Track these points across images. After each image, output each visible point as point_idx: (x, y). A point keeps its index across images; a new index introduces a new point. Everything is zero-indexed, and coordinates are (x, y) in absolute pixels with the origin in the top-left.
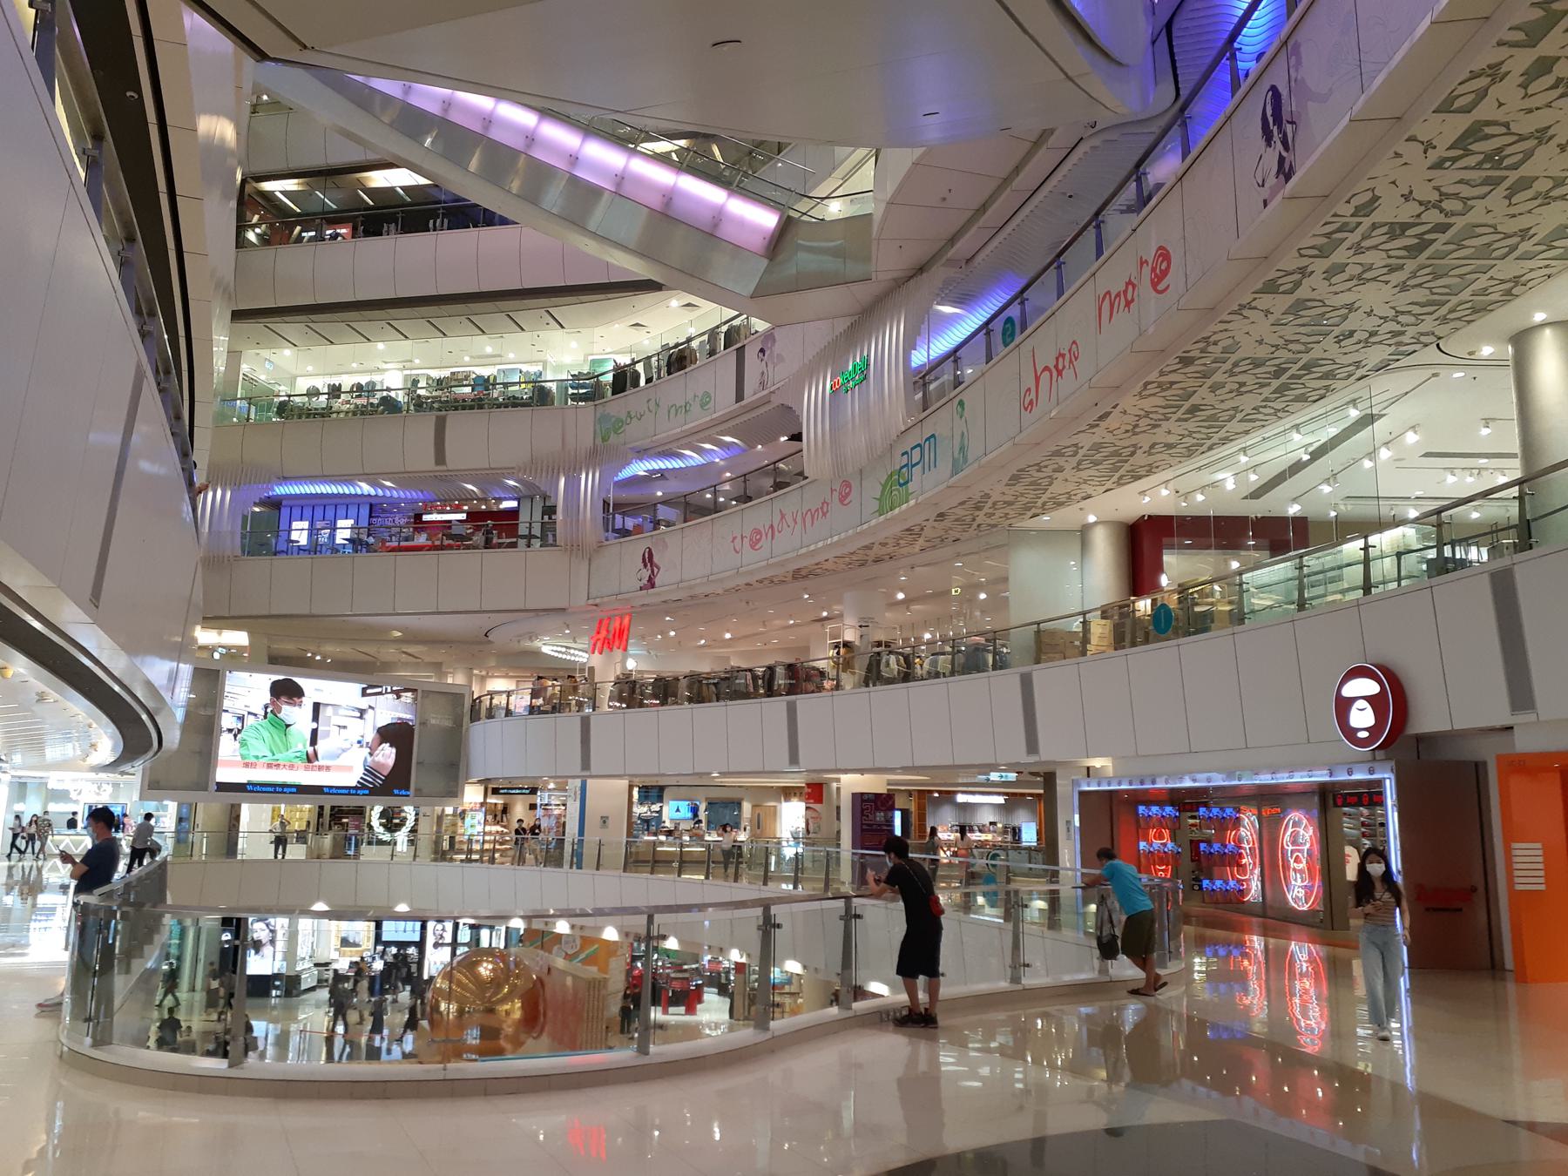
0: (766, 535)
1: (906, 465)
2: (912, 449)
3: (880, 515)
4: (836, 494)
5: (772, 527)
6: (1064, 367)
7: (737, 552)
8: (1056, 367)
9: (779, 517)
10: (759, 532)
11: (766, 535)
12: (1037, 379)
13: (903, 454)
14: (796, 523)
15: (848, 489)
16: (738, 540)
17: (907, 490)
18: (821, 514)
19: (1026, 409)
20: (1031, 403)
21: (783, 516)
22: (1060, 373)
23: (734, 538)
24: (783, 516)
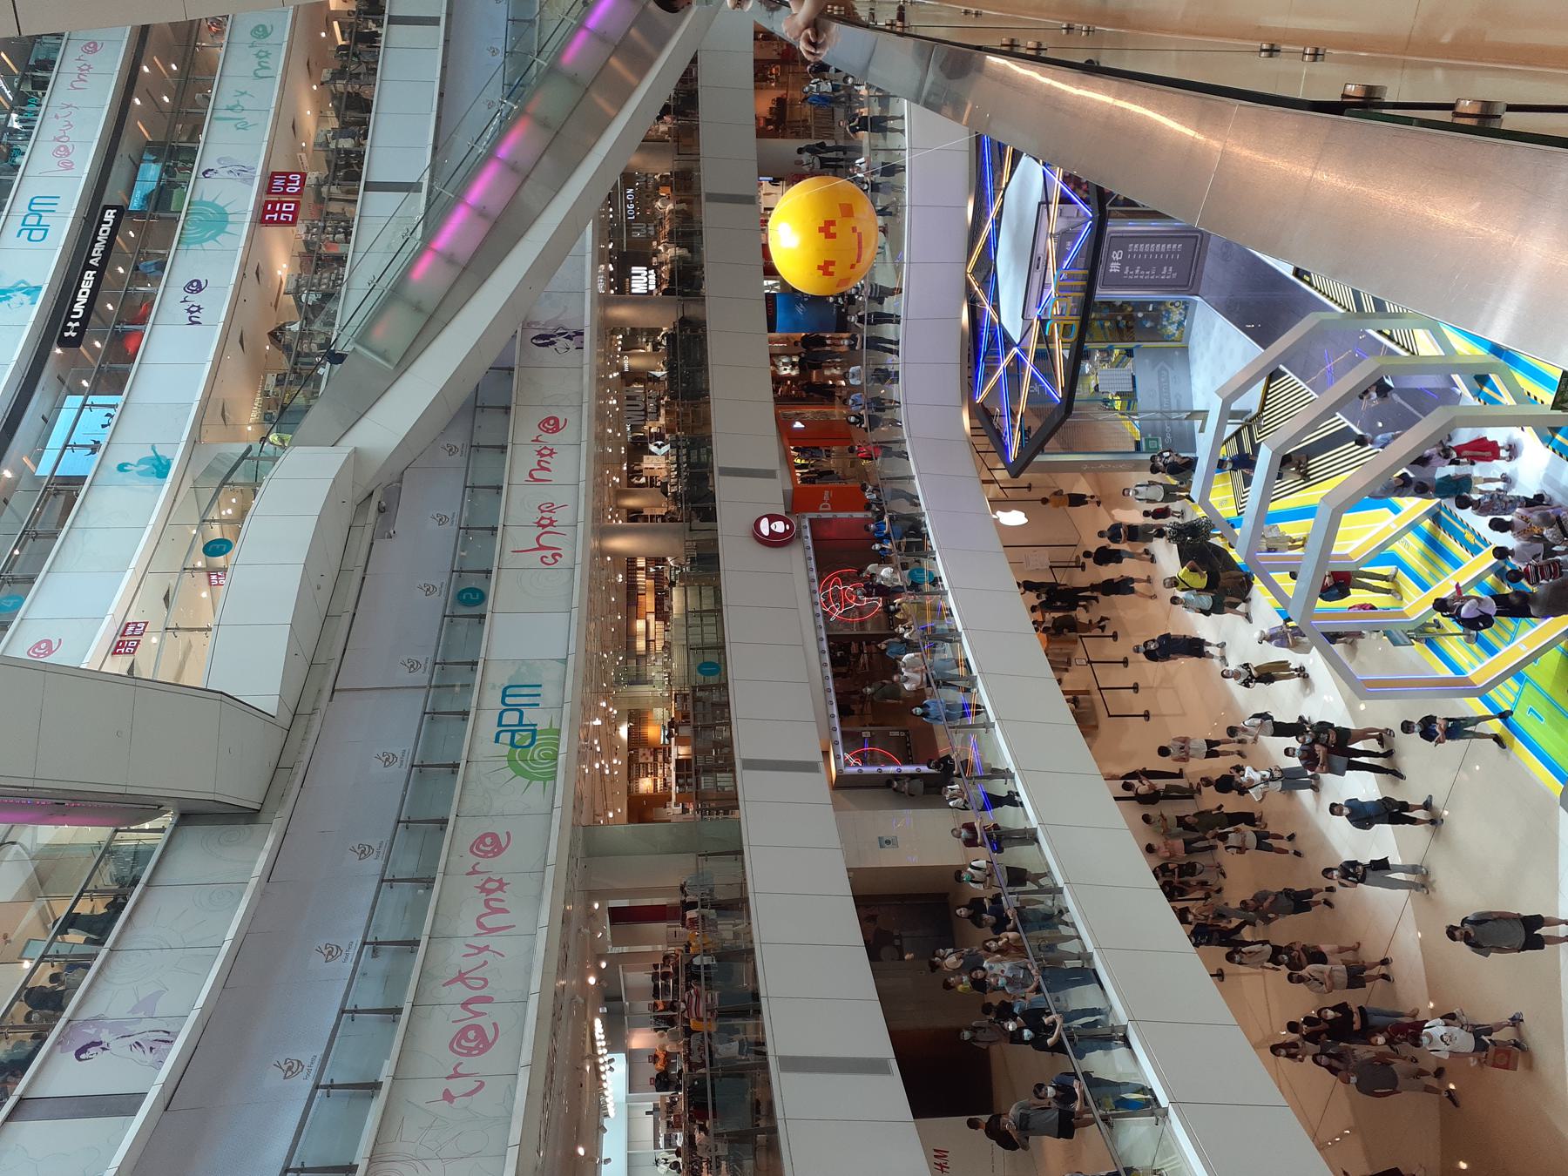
0: (477, 1014)
1: (513, 733)
2: (500, 724)
3: (554, 778)
4: (484, 864)
5: (465, 1005)
6: (550, 519)
7: (482, 1084)
8: (544, 526)
9: (459, 985)
10: (463, 1033)
11: (477, 1014)
12: (542, 548)
13: (497, 741)
14: (486, 948)
15: (488, 840)
16: (457, 1087)
17: (545, 732)
18: (498, 895)
19: (556, 561)
20: (553, 556)
21: (461, 977)
22: (552, 523)
23: (448, 1096)
24: (461, 977)
